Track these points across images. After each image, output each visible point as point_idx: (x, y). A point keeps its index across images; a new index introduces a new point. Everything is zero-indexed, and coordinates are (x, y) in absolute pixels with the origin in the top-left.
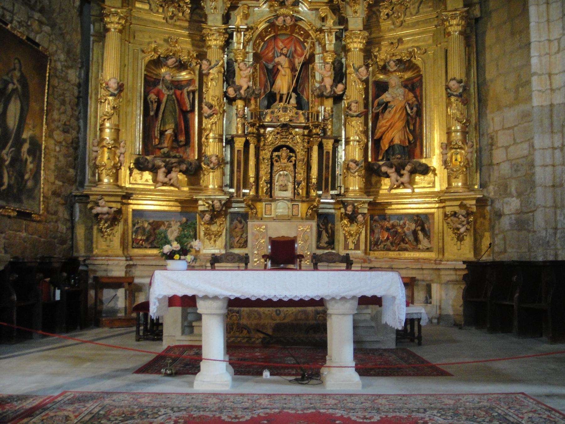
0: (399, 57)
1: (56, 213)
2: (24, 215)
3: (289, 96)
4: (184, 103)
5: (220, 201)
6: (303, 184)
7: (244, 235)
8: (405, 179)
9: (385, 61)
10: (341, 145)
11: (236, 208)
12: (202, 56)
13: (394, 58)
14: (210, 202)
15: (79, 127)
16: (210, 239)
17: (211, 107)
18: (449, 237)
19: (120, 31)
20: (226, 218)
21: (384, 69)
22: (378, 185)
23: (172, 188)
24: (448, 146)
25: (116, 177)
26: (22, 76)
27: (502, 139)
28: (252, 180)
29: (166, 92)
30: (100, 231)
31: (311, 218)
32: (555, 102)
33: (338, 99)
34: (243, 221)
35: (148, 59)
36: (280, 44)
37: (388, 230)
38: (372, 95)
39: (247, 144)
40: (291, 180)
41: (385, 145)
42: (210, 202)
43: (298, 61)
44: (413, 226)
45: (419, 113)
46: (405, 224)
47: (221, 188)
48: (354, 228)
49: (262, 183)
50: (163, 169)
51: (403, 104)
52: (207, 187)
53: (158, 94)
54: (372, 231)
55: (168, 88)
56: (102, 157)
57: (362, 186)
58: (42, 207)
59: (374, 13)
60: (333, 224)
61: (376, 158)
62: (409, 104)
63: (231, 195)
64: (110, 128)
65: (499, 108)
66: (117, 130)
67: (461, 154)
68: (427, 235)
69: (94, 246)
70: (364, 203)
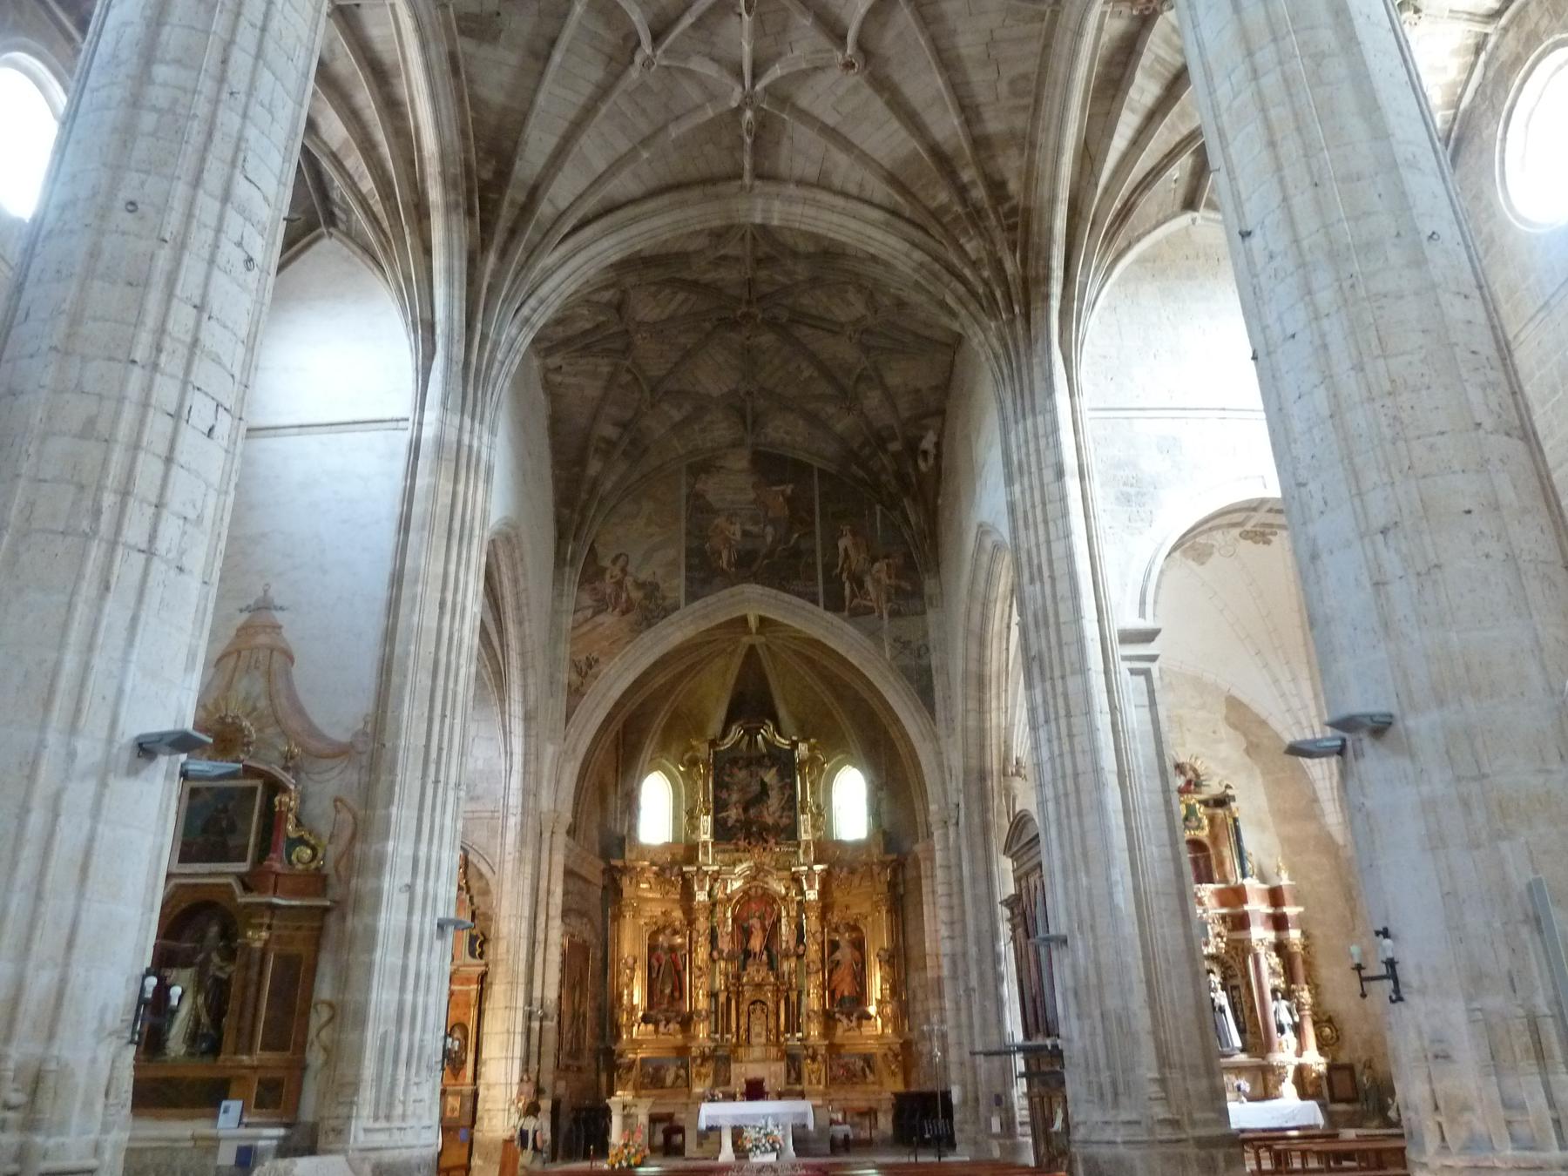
8: (854, 1024)
11: (720, 1053)
17: (700, 969)
22: (835, 1027)
24: (880, 1003)
27: (920, 995)
28: (734, 1029)
31: (781, 1059)
33: (799, 957)
37: (843, 1066)
39: (728, 1000)
41: (838, 996)
44: (862, 1063)
47: (708, 1035)
49: (741, 1031)
50: (664, 1023)
61: (831, 1005)
63: (716, 1040)
68: (872, 1071)
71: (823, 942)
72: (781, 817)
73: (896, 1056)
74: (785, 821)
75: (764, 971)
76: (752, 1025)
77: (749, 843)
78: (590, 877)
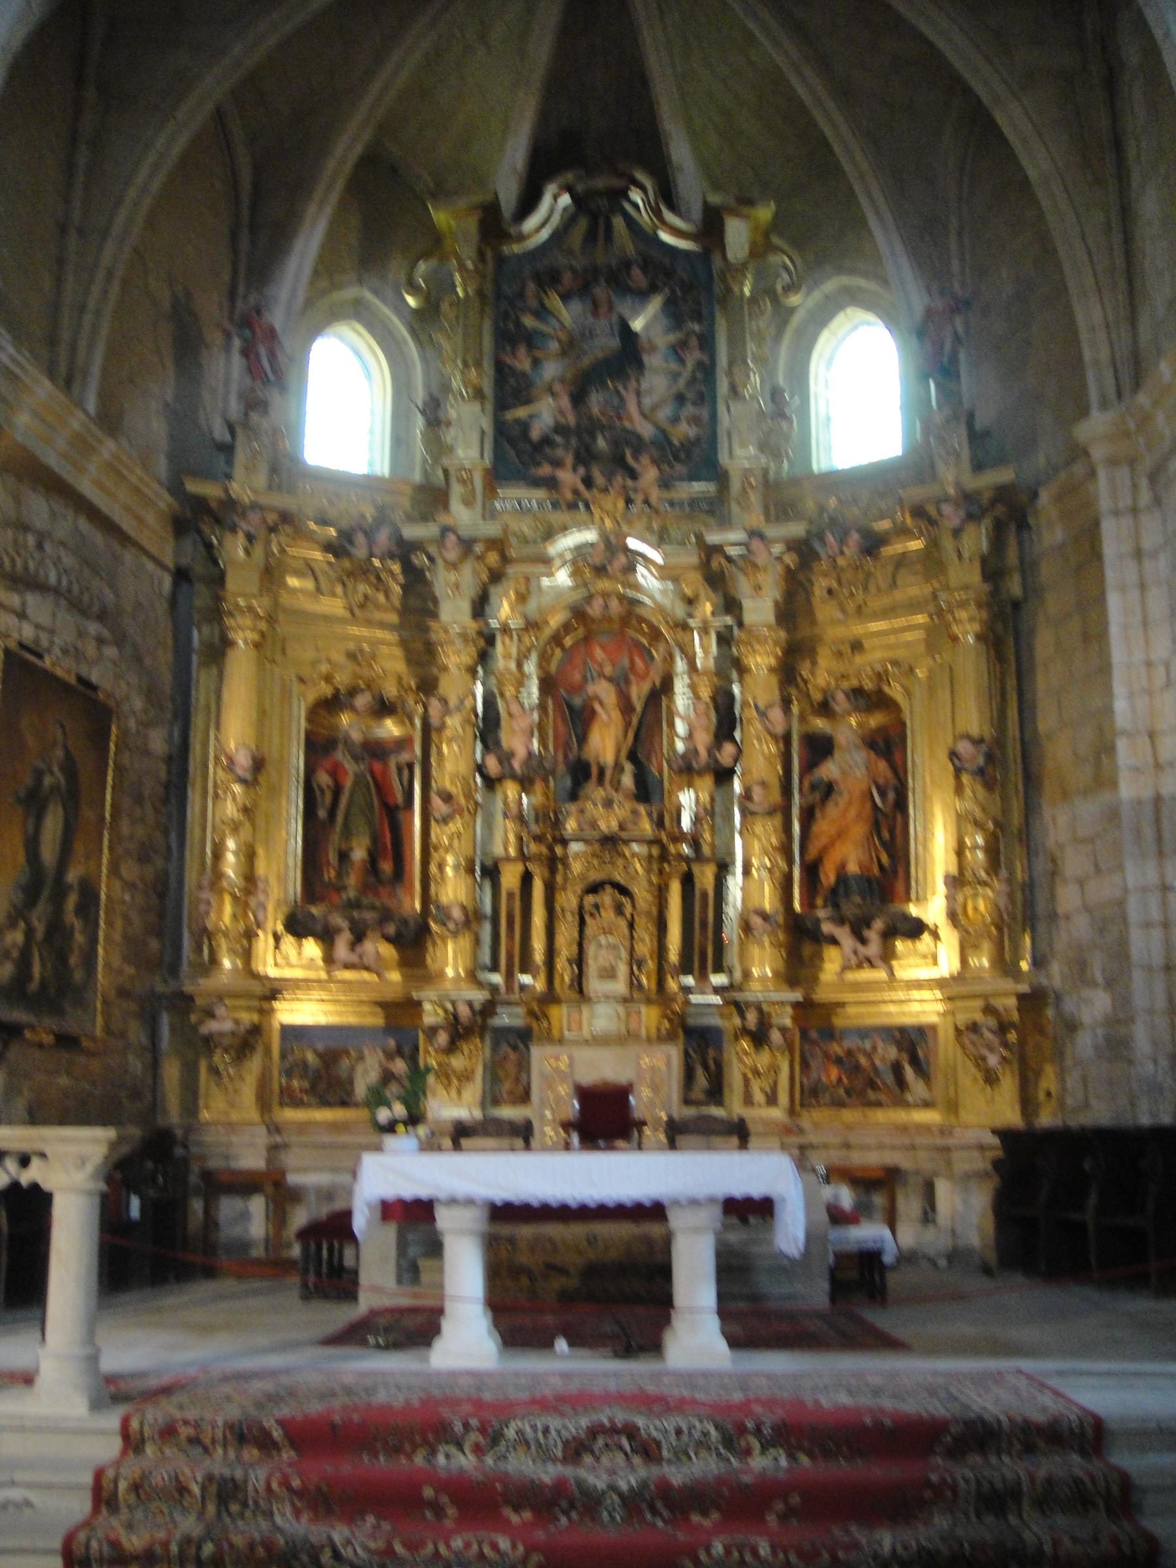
0: (855, 683)
1: (123, 1035)
2: (67, 1041)
3: (618, 768)
4: (391, 787)
5: (470, 1004)
6: (651, 965)
7: (524, 1076)
8: (873, 948)
9: (824, 692)
10: (734, 874)
11: (505, 1018)
12: (428, 687)
13: (845, 685)
14: (449, 1006)
15: (169, 848)
16: (448, 1086)
17: (447, 798)
18: (968, 1078)
19: (257, 646)
20: (482, 1038)
21: (825, 708)
23: (366, 976)
24: (956, 882)
25: (247, 955)
26: (69, 756)
27: (1074, 863)
29: (351, 768)
30: (215, 1071)
31: (670, 1037)
32: (1165, 791)
33: (723, 776)
34: (521, 1046)
35: (312, 696)
36: (599, 654)
37: (839, 1061)
38: (800, 763)
39: (527, 879)
40: (624, 954)
41: (828, 876)
42: (449, 1006)
43: (638, 693)
44: (892, 1053)
45: (901, 804)
46: (874, 1048)
47: (472, 976)
48: (763, 1059)
49: (561, 964)
51: (864, 786)
52: (442, 974)
53: (336, 772)
54: (805, 1065)
55: (356, 758)
56: (220, 911)
57: (780, 965)
58: (99, 1020)
59: (801, 584)
60: (719, 1049)
62: (878, 787)
63: (494, 989)
64: (236, 853)
65: (1065, 795)
66: (249, 855)
67: (985, 897)
69: (201, 1102)
70: (782, 1003)
71: (787, 739)
72: (675, 420)
73: (1003, 1028)
74: (684, 430)
75: (622, 810)
76: (591, 950)
77: (588, 482)
78: (127, 524)
